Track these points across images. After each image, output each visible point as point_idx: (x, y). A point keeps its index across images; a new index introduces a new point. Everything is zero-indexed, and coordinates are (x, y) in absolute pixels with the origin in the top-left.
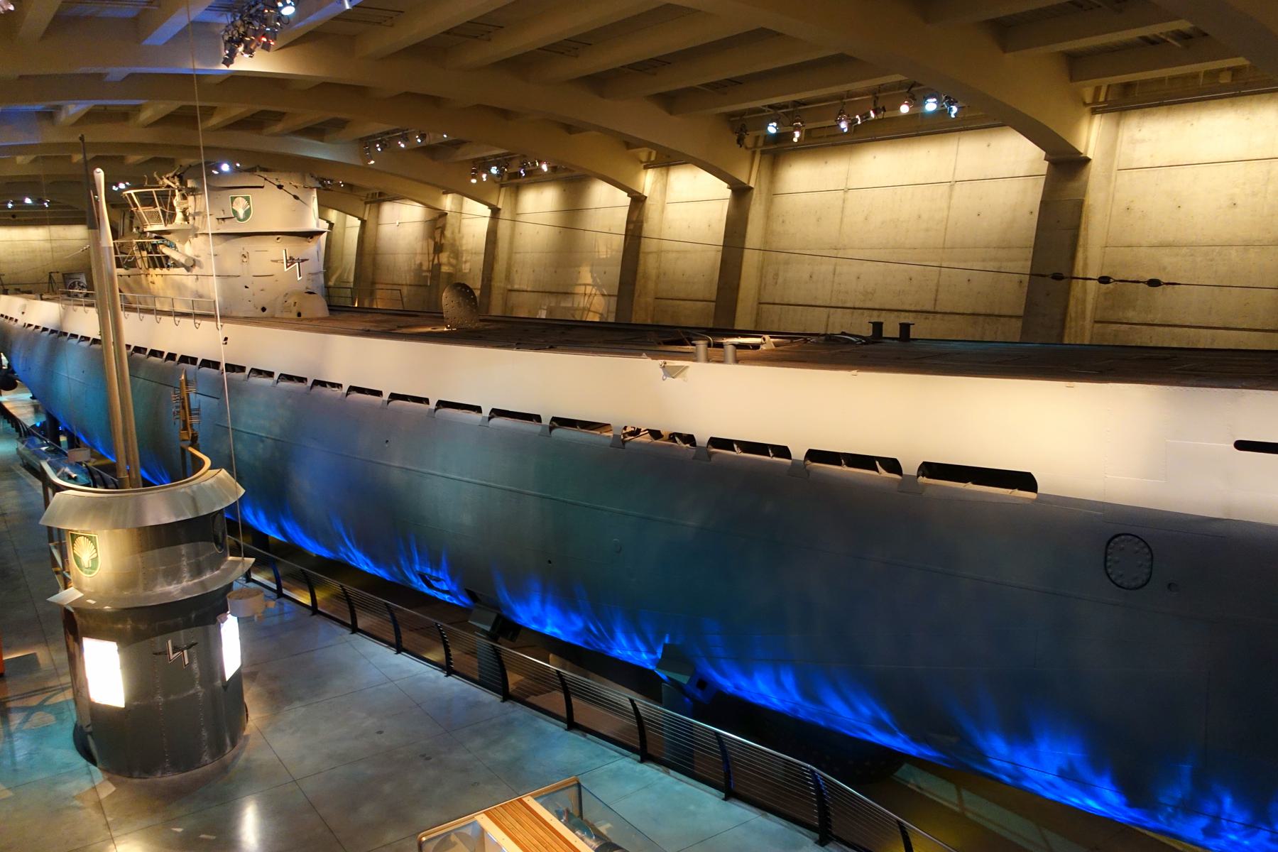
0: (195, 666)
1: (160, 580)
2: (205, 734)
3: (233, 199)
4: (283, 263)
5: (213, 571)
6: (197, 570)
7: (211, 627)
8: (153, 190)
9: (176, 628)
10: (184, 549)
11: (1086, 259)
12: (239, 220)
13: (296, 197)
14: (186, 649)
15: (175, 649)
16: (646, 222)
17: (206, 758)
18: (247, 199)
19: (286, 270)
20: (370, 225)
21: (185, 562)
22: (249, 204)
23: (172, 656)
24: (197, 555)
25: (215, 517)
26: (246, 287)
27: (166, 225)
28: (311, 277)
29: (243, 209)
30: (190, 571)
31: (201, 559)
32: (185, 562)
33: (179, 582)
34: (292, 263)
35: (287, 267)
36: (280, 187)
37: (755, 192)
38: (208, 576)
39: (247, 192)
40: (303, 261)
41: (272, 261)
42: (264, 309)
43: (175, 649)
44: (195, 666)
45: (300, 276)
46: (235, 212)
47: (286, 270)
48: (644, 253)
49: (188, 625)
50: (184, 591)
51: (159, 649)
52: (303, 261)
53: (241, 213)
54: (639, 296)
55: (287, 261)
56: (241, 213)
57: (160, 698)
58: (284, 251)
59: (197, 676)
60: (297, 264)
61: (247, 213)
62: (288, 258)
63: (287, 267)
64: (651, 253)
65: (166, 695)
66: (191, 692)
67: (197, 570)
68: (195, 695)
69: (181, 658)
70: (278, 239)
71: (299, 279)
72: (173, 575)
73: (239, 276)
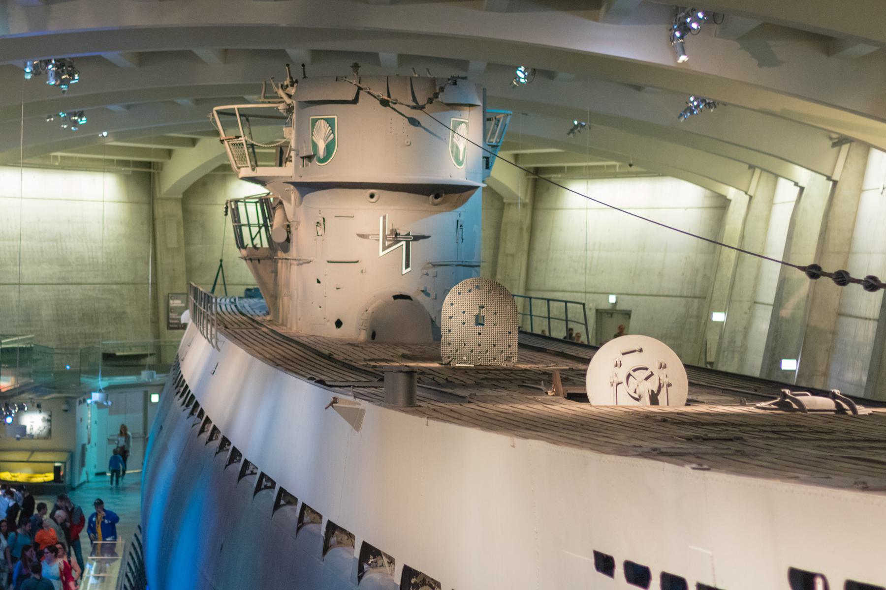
3: (315, 121)
4: (378, 240)
8: (236, 107)
13: (413, 122)
18: (331, 123)
19: (381, 253)
22: (333, 132)
26: (319, 282)
27: (253, 170)
28: (432, 271)
35: (384, 248)
36: (384, 103)
39: (332, 112)
40: (417, 238)
41: (359, 235)
42: (339, 324)
45: (407, 266)
46: (315, 146)
47: (381, 253)
52: (417, 238)
53: (322, 146)
55: (385, 238)
56: (322, 146)
58: (381, 219)
60: (404, 243)
61: (330, 148)
63: (384, 248)
70: (372, 196)
71: (405, 271)
73: (357, 262)
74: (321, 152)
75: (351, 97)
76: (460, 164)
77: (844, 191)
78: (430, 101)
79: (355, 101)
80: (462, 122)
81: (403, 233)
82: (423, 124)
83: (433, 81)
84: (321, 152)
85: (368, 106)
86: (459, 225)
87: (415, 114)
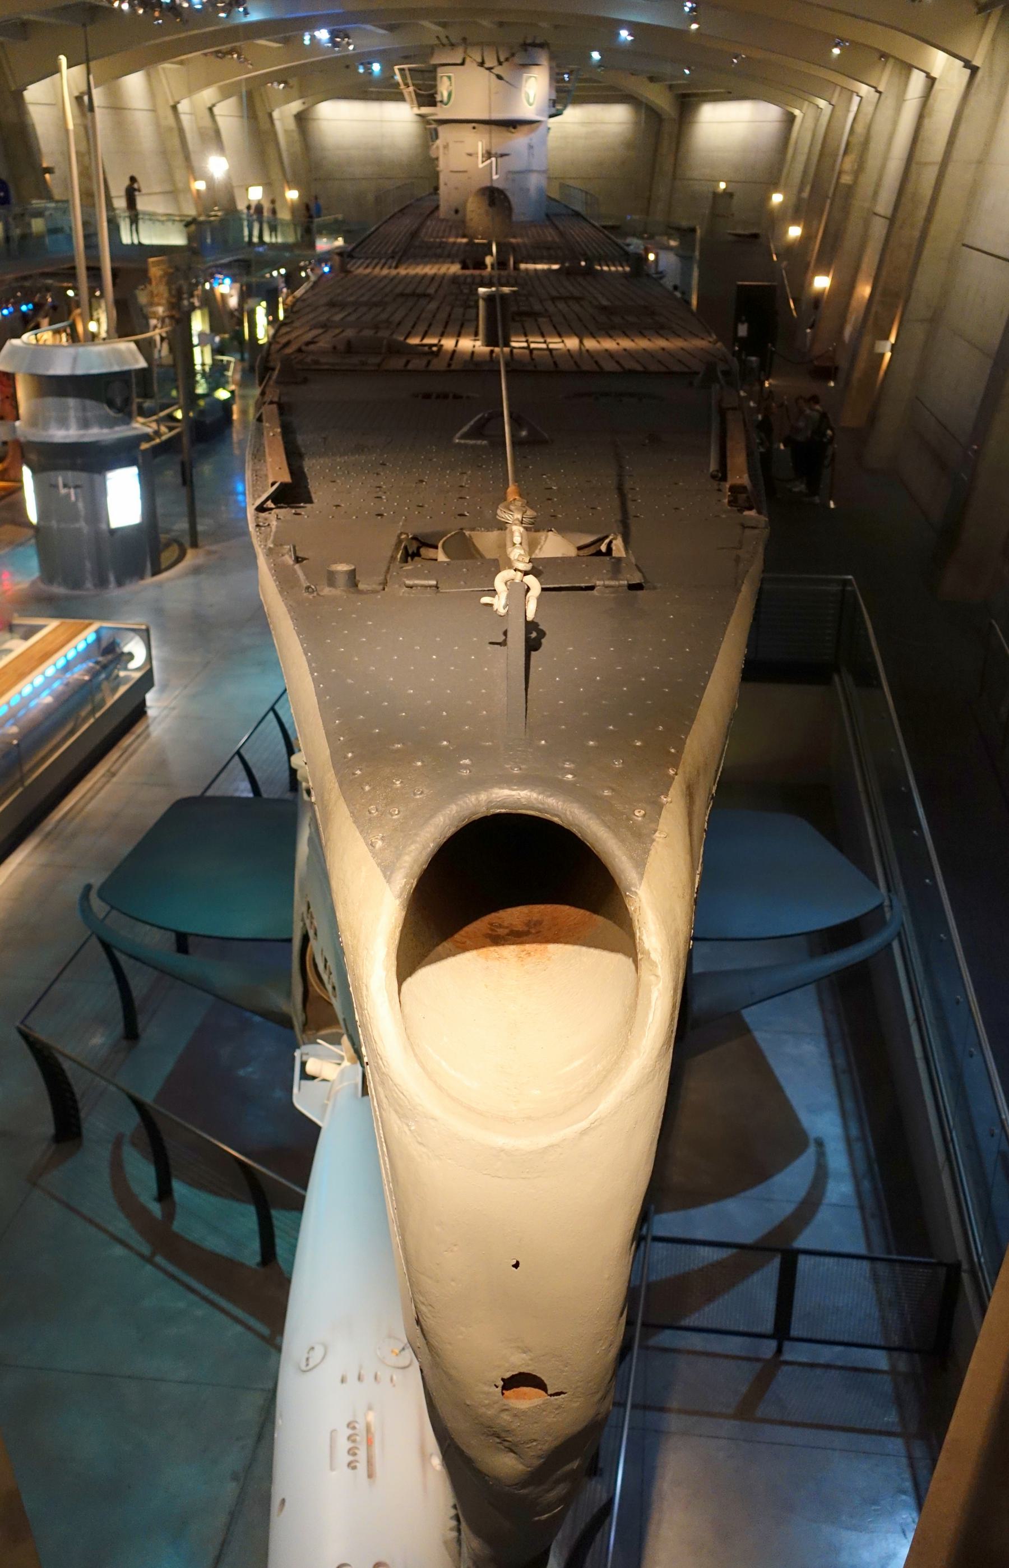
0: (81, 505)
2: (88, 565)
5: (101, 427)
6: (85, 424)
7: (97, 477)
10: (71, 402)
12: (446, 104)
13: (499, 77)
15: (65, 486)
18: (449, 78)
19: (481, 166)
20: (839, 113)
21: (72, 413)
23: (63, 491)
24: (84, 409)
29: (447, 90)
32: (72, 413)
33: (67, 428)
34: (490, 158)
35: (483, 162)
40: (502, 155)
43: (65, 486)
44: (81, 505)
45: (496, 174)
48: (917, 163)
49: (73, 468)
50: (66, 437)
52: (502, 155)
53: (445, 94)
54: (901, 227)
55: (483, 157)
57: (54, 524)
60: (493, 159)
62: (484, 152)
63: (483, 162)
66: (77, 525)
67: (85, 424)
69: (68, 495)
72: (63, 423)
75: (459, 61)
76: (531, 105)
79: (463, 64)
80: (531, 77)
81: (493, 152)
82: (505, 78)
84: (445, 99)
85: (471, 67)
86: (531, 147)
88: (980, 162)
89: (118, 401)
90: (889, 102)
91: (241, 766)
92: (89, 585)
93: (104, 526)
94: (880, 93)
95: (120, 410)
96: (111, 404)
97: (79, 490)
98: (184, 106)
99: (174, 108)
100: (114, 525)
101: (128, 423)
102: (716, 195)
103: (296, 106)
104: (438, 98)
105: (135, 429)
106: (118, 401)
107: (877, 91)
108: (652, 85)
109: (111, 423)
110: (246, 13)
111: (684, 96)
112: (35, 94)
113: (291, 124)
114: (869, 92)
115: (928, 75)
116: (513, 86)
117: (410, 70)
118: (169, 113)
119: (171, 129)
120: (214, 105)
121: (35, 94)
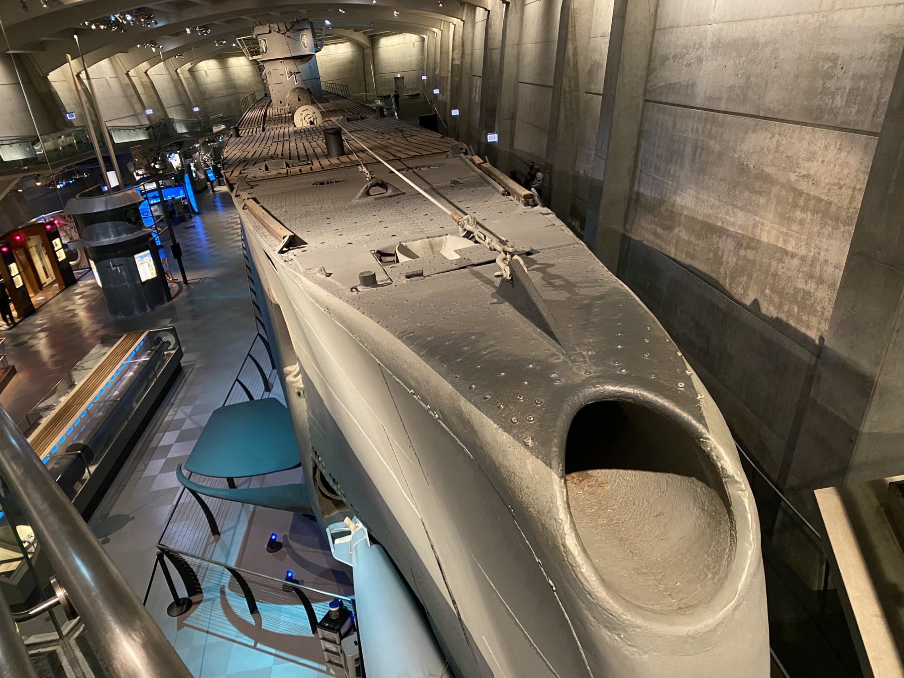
0: (124, 274)
1: (101, 236)
9: (112, 257)
10: (109, 224)
11: (575, 48)
13: (289, 37)
14: (119, 266)
16: (491, 28)
17: (136, 312)
18: (264, 40)
24: (116, 227)
25: (126, 212)
30: (114, 233)
31: (119, 228)
37: (511, 5)
38: (124, 236)
40: (297, 73)
44: (124, 274)
49: (117, 256)
51: (107, 265)
52: (297, 73)
53: (264, 48)
59: (126, 278)
64: (495, 49)
65: (114, 285)
66: (124, 284)
67: (118, 234)
68: (126, 286)
72: (107, 235)
74: (265, 51)
77: (445, 33)
78: (291, 28)
79: (270, 32)
83: (292, 22)
84: (265, 51)
87: (288, 34)
88: (518, 44)
89: (133, 220)
90: (469, 25)
91: (240, 386)
92: (136, 312)
93: (138, 282)
94: (464, 21)
95: (135, 224)
96: (130, 221)
97: (121, 267)
98: (131, 73)
99: (127, 74)
100: (143, 280)
101: (141, 229)
102: (396, 79)
103: (188, 66)
104: (261, 51)
105: (145, 231)
106: (133, 220)
107: (462, 21)
108: (356, 33)
109: (131, 231)
110: (156, 23)
111: (371, 36)
112: (53, 76)
113: (188, 75)
114: (458, 22)
115: (486, 9)
116: (297, 40)
117: (244, 39)
118: (125, 77)
119: (128, 84)
120: (147, 70)
121: (53, 76)
